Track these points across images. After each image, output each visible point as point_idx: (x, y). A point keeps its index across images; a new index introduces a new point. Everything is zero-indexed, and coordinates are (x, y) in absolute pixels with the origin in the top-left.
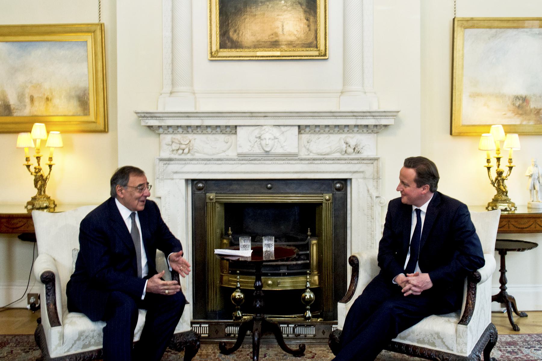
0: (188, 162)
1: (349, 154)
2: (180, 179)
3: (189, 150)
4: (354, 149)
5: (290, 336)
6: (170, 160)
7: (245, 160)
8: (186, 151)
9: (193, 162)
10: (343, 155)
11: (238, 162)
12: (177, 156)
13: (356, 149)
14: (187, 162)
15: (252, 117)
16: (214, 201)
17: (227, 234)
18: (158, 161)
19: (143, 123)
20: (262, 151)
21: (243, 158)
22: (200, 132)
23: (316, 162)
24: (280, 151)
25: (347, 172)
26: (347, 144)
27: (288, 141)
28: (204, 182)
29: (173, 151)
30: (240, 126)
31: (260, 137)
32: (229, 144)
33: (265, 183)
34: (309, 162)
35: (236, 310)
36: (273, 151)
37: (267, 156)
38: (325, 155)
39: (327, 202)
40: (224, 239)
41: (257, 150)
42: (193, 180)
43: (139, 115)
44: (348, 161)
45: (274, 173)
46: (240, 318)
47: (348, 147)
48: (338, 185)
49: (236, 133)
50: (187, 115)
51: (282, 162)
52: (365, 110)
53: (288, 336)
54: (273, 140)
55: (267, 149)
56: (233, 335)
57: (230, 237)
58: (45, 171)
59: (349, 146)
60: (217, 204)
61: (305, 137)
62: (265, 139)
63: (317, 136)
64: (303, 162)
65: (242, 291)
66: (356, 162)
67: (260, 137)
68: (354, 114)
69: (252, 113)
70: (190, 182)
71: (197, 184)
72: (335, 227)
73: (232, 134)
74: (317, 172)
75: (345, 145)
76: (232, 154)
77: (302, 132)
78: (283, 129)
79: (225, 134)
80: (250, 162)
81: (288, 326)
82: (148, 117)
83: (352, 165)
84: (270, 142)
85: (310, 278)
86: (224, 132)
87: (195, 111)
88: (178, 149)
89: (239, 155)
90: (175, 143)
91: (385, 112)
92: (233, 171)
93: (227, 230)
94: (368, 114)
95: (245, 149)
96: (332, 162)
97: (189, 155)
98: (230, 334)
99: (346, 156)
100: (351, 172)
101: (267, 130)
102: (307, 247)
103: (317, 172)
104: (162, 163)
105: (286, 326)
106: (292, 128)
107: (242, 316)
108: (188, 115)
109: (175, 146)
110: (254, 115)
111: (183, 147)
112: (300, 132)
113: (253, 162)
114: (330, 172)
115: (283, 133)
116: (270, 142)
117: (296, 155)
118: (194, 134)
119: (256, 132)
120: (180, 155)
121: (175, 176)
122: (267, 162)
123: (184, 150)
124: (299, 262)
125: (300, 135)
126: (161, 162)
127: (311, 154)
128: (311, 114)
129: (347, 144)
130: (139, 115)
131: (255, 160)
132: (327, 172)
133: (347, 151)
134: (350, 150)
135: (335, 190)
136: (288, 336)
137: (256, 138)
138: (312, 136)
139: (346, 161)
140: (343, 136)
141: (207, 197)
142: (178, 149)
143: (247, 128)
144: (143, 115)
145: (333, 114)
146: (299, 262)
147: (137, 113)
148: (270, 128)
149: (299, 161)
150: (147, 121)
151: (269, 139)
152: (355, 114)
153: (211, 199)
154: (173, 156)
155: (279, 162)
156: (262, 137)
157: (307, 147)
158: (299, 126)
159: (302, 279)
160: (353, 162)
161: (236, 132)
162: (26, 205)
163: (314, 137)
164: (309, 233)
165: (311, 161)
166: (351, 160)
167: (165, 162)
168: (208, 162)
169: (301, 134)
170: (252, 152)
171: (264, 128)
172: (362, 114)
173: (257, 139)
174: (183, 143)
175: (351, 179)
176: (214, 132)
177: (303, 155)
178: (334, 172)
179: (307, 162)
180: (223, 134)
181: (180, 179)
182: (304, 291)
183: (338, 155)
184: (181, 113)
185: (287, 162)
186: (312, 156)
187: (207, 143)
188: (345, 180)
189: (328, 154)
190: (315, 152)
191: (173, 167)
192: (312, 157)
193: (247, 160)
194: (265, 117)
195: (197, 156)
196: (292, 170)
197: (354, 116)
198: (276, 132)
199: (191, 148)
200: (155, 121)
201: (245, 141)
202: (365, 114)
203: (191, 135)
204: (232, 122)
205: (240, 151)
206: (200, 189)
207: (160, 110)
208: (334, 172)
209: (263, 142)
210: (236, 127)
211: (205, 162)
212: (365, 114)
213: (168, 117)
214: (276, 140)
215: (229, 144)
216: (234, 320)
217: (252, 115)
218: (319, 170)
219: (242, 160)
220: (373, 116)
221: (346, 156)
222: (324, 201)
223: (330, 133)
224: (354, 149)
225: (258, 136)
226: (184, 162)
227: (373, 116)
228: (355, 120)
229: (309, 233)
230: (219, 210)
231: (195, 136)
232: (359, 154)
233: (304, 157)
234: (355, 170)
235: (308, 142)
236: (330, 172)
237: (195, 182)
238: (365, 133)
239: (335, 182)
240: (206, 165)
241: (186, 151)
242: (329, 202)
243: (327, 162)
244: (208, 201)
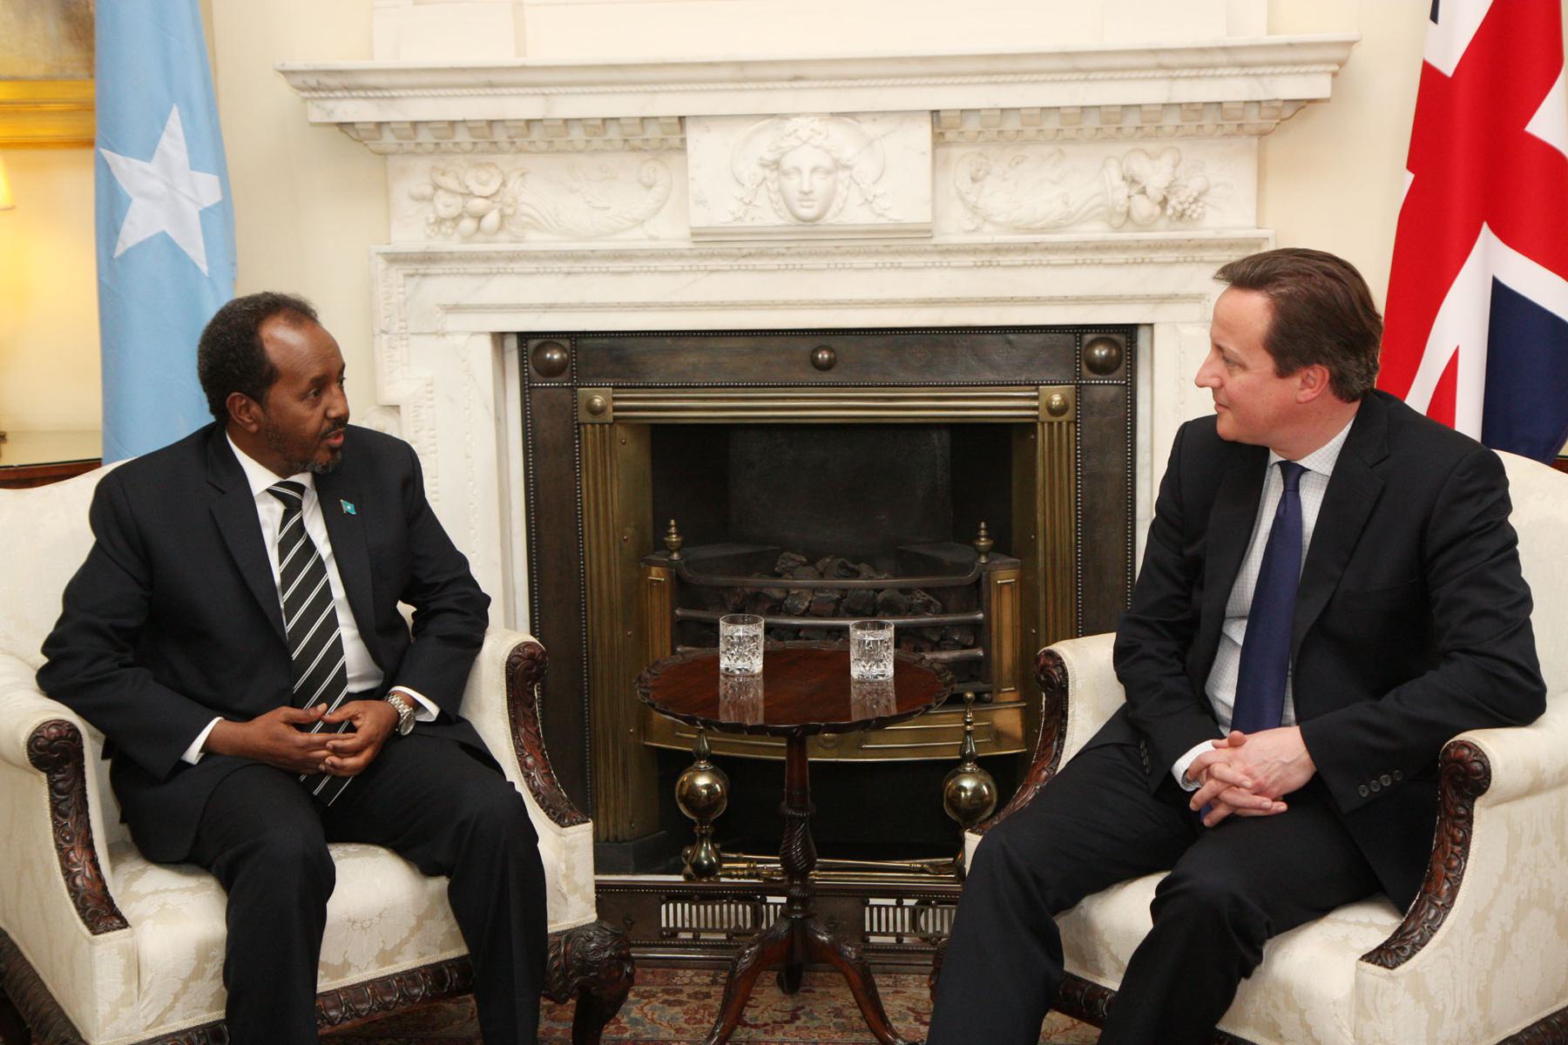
0: (502, 265)
1: (1143, 227)
2: (474, 334)
3: (503, 217)
4: (1164, 203)
5: (906, 940)
6: (429, 258)
7: (720, 256)
8: (492, 219)
9: (517, 266)
10: (1118, 229)
11: (694, 262)
12: (454, 245)
13: (1173, 202)
14: (495, 266)
15: (746, 80)
16: (610, 415)
17: (661, 545)
18: (381, 264)
19: (316, 115)
20: (789, 219)
21: (714, 247)
22: (543, 146)
23: (1005, 260)
24: (853, 214)
26: (1133, 181)
27: (891, 178)
28: (566, 343)
29: (440, 221)
31: (776, 165)
33: (806, 345)
34: (978, 259)
35: (694, 841)
36: (830, 218)
37: (810, 239)
38: (1042, 230)
39: (1054, 419)
40: (652, 563)
41: (767, 216)
42: (524, 337)
43: (298, 80)
44: (1139, 255)
46: (710, 871)
47: (1138, 199)
48: (1100, 352)
49: (682, 148)
50: (484, 78)
51: (871, 261)
52: (1205, 42)
53: (899, 941)
54: (828, 172)
56: (683, 936)
57: (675, 556)
59: (1143, 192)
60: (621, 432)
61: (961, 159)
62: (798, 170)
64: (955, 260)
65: (720, 765)
66: (1170, 256)
67: (776, 165)
68: (1161, 61)
69: (741, 65)
70: (512, 344)
71: (540, 349)
72: (1089, 519)
73: (671, 149)
74: (1013, 301)
75: (1120, 193)
76: (670, 232)
77: (950, 136)
78: (870, 128)
80: (742, 262)
81: (900, 904)
82: (331, 90)
83: (1151, 270)
84: (820, 184)
85: (977, 718)
86: (637, 143)
87: (519, 62)
88: (460, 216)
89: (696, 234)
90: (448, 191)
91: (1291, 45)
92: (676, 299)
93: (661, 529)
94: (1221, 58)
95: (721, 212)
96: (1070, 258)
97: (503, 236)
98: (674, 933)
99: (1126, 236)
100: (1148, 299)
102: (976, 593)
103: (1013, 301)
104: (397, 274)
105: (893, 902)
107: (721, 860)
108: (489, 79)
109: (446, 205)
110: (751, 72)
111: (478, 205)
112: (939, 138)
113: (752, 262)
114: (1065, 300)
115: (870, 143)
116: (820, 184)
117: (925, 232)
118: (520, 151)
120: (467, 238)
121: (453, 322)
122: (808, 262)
123: (480, 218)
124: (945, 656)
125: (941, 151)
126: (395, 267)
127: (988, 228)
128: (984, 66)
129: (1133, 181)
130: (298, 80)
131: (761, 254)
133: (1135, 214)
135: (1084, 368)
136: (899, 941)
137: (764, 166)
139: (1129, 256)
141: (582, 403)
142: (460, 216)
144: (312, 82)
145: (1075, 64)
146: (945, 656)
147: (287, 73)
148: (817, 125)
149: (937, 258)
150: (330, 105)
151: (814, 170)
152: (1167, 60)
153: (595, 411)
154: (439, 244)
156: (787, 164)
157: (972, 198)
158: (935, 113)
159: (948, 720)
160: (1158, 256)
161: (683, 140)
164: (983, 542)
165: (986, 258)
166: (1148, 247)
167: (410, 269)
168: (578, 266)
169: (948, 144)
170: (748, 222)
172: (1196, 59)
173: (767, 172)
174: (476, 188)
175: (1151, 325)
176: (597, 142)
177: (955, 228)
178: (1079, 300)
179: (969, 260)
180: (634, 149)
181: (474, 334)
182: (952, 768)
183: (1095, 231)
184: (463, 70)
185: (888, 259)
186: (991, 236)
188: (1130, 331)
189: (1056, 227)
190: (998, 219)
191: (443, 287)
192: (988, 239)
193: (730, 256)
194: (797, 78)
195: (536, 241)
196: (911, 293)
197: (1161, 67)
198: (841, 139)
199: (509, 211)
200: (361, 104)
201: (722, 178)
202: (1207, 59)
203: (508, 157)
204: (667, 105)
205: (701, 219)
206: (551, 371)
207: (383, 60)
208: (1079, 300)
210: (681, 119)
211: (565, 266)
212: (1207, 59)
213: (412, 87)
214: (842, 175)
216: (688, 877)
217: (744, 73)
218: (1021, 293)
219: (712, 256)
220: (1243, 66)
222: (1044, 415)
223: (1066, 140)
224: (1164, 203)
225: (769, 157)
226: (482, 267)
227: (1243, 66)
228: (1164, 83)
229: (983, 542)
230: (630, 454)
232: (1180, 225)
233: (956, 239)
234: (1167, 289)
235: (974, 180)
236: (1065, 300)
237: (533, 343)
238: (1210, 136)
239: (1089, 337)
240: (571, 280)
241: (492, 219)
242: (1064, 418)
243: (1055, 258)
244: (584, 416)
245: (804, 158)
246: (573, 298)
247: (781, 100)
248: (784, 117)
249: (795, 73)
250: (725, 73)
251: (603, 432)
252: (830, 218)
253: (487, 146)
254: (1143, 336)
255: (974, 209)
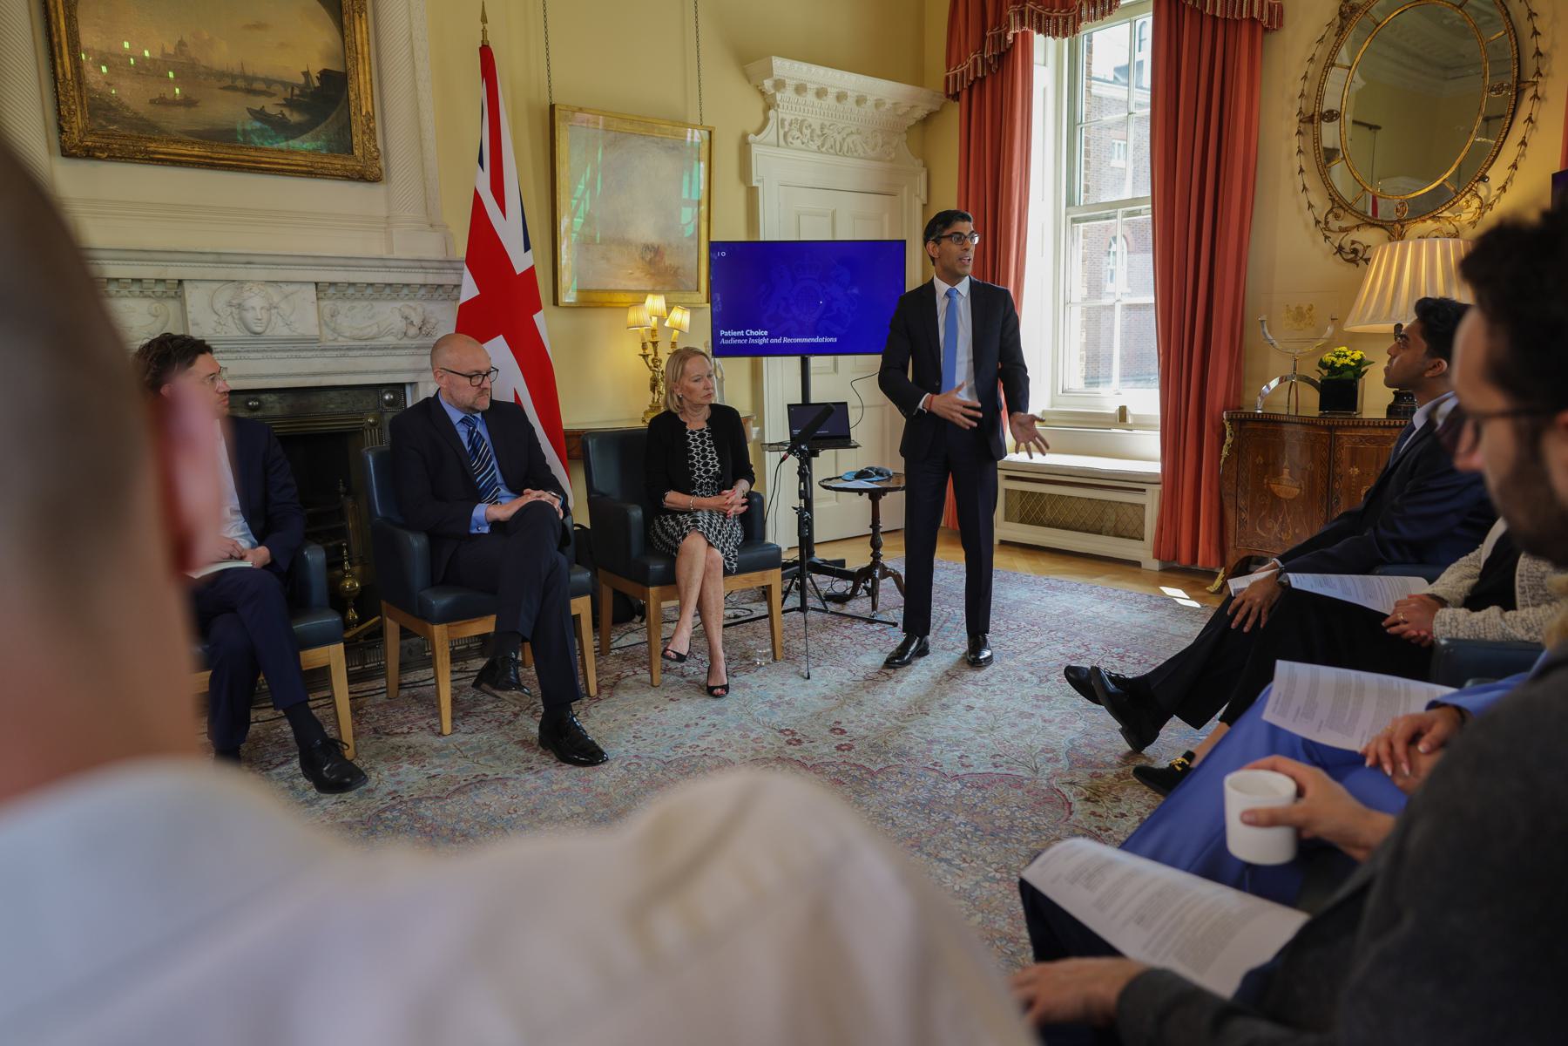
25: (409, 371)
31: (240, 306)
36: (268, 332)
45: (267, 376)
55: (258, 329)
63: (348, 304)
67: (240, 306)
99: (405, 341)
100: (414, 371)
101: (255, 289)
106: (304, 287)
110: (224, 258)
119: (226, 293)
122: (252, 355)
132: (373, 372)
134: (413, 331)
138: (339, 303)
140: (399, 304)
155: (278, 355)
156: (249, 304)
163: (343, 306)
171: (247, 286)
179: (334, 353)
204: (173, 273)
208: (386, 372)
209: (249, 316)
210: (180, 282)
217: (220, 258)
221: (405, 341)
245: (255, 301)
247: (240, 273)
248: (242, 282)
249: (248, 260)
250: (210, 258)
252: (268, 332)
254: (408, 389)
255: (334, 330)
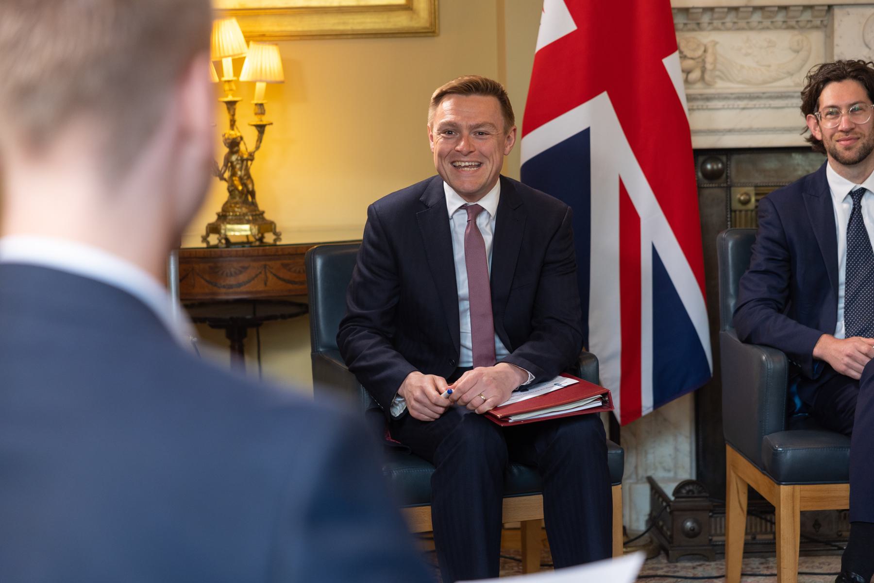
22: (729, 25)
28: (724, 158)
30: (841, 5)
32: (803, 54)
58: (248, 144)
79: (792, 28)
86: (793, 23)
143: (861, 10)
162: (204, 232)
168: (751, 103)
187: (747, 54)
210: (830, 7)
211: (742, 104)
215: (803, 54)
231: (715, 36)
240: (746, 112)
244: (736, 206)
246: (744, 124)
251: (746, 215)
253: (695, 26)
